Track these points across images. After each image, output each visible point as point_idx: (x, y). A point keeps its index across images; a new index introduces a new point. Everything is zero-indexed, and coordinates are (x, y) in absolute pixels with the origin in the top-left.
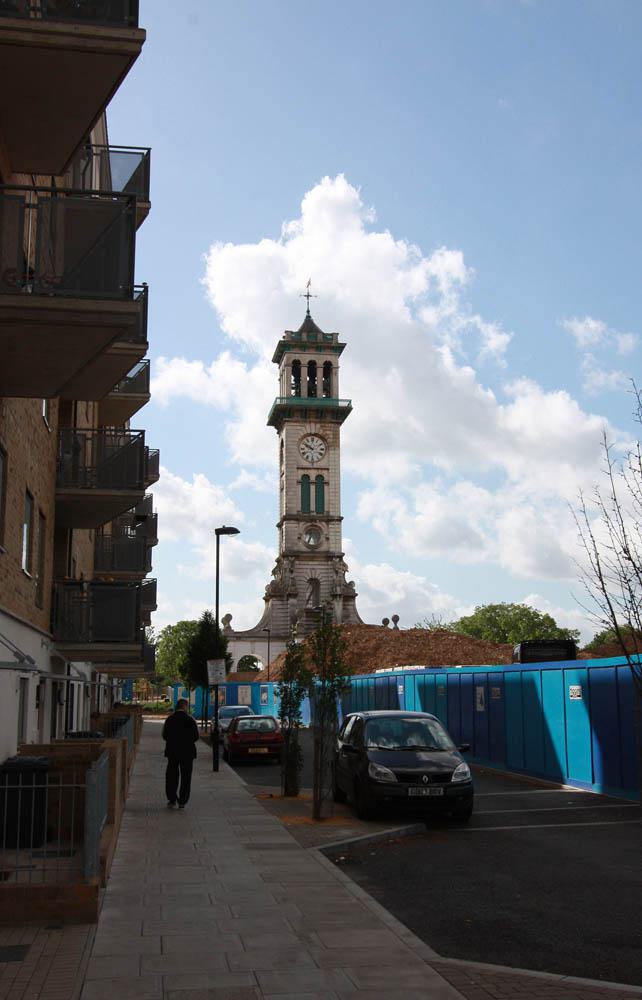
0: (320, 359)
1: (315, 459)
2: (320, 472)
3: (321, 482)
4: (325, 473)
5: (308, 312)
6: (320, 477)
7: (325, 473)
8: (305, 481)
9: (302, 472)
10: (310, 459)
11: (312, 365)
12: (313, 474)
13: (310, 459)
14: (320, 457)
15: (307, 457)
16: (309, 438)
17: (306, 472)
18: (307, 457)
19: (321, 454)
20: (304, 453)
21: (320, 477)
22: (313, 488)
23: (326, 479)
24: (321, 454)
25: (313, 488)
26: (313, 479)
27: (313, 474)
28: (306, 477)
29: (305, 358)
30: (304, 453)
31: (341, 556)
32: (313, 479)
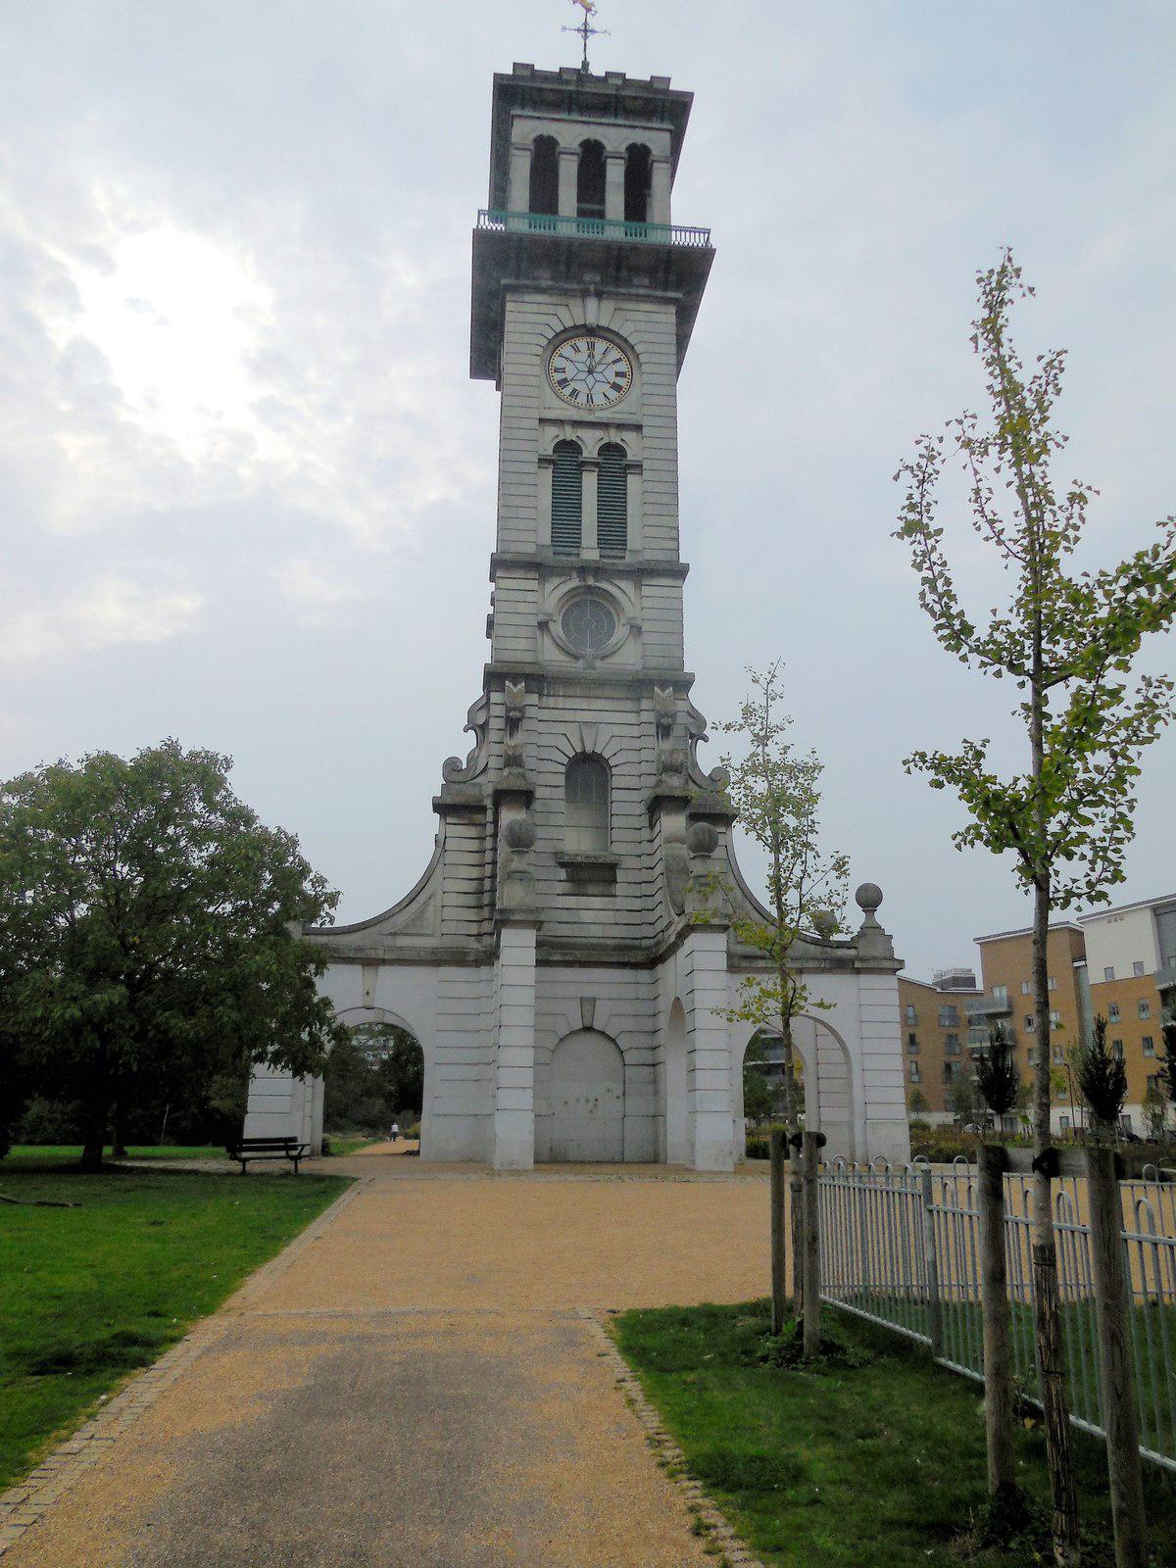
0: (616, 137)
1: (599, 400)
2: (614, 436)
3: (615, 463)
6: (612, 450)
8: (565, 459)
9: (550, 436)
10: (582, 399)
12: (591, 444)
13: (582, 399)
14: (613, 394)
15: (574, 393)
16: (582, 343)
18: (574, 393)
19: (617, 387)
20: (563, 383)
21: (612, 450)
22: (590, 481)
23: (632, 456)
25: (590, 481)
26: (590, 451)
27: (591, 444)
28: (568, 448)
29: (570, 134)
30: (563, 383)
31: (684, 684)
32: (590, 451)
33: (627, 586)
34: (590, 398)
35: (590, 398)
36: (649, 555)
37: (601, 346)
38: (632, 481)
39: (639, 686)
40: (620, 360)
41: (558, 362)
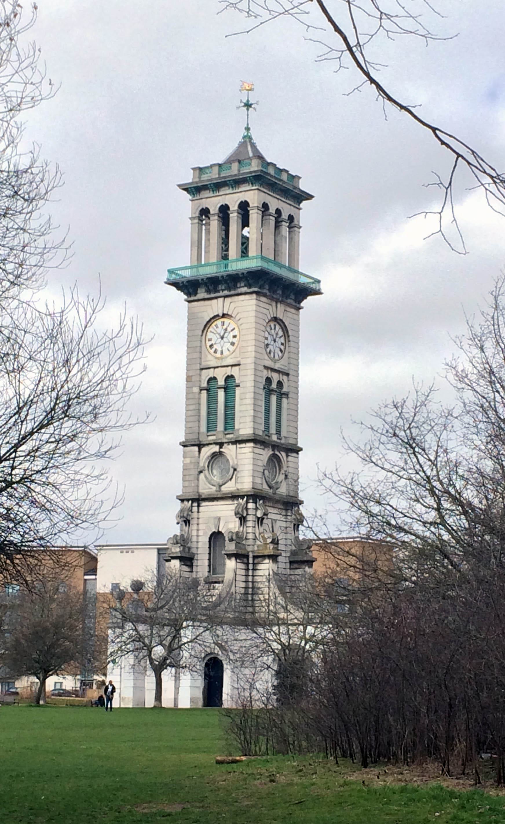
1: (226, 353)
2: (229, 371)
4: (235, 371)
5: (248, 129)
6: (229, 378)
7: (235, 371)
9: (207, 374)
10: (218, 355)
11: (224, 210)
13: (219, 352)
14: (232, 348)
15: (215, 352)
16: (219, 322)
17: (211, 373)
19: (233, 344)
20: (211, 346)
23: (237, 381)
24: (233, 344)
25: (221, 394)
26: (221, 382)
27: (221, 375)
33: (232, 447)
34: (222, 353)
35: (222, 353)
36: (242, 432)
37: (226, 321)
38: (238, 391)
39: (234, 497)
40: (234, 329)
41: (210, 335)
